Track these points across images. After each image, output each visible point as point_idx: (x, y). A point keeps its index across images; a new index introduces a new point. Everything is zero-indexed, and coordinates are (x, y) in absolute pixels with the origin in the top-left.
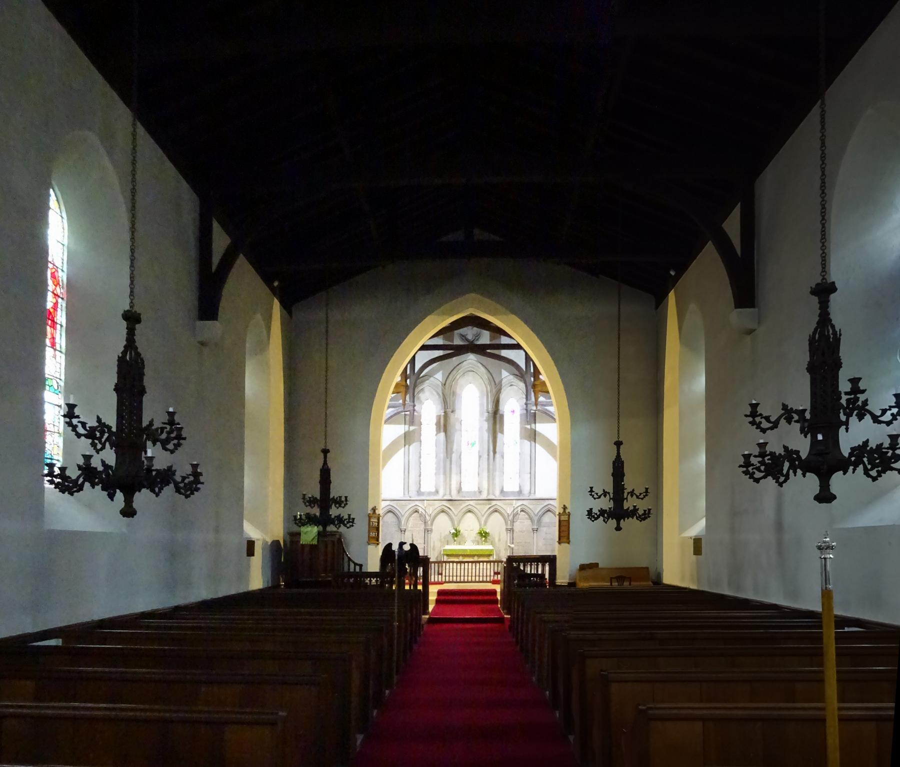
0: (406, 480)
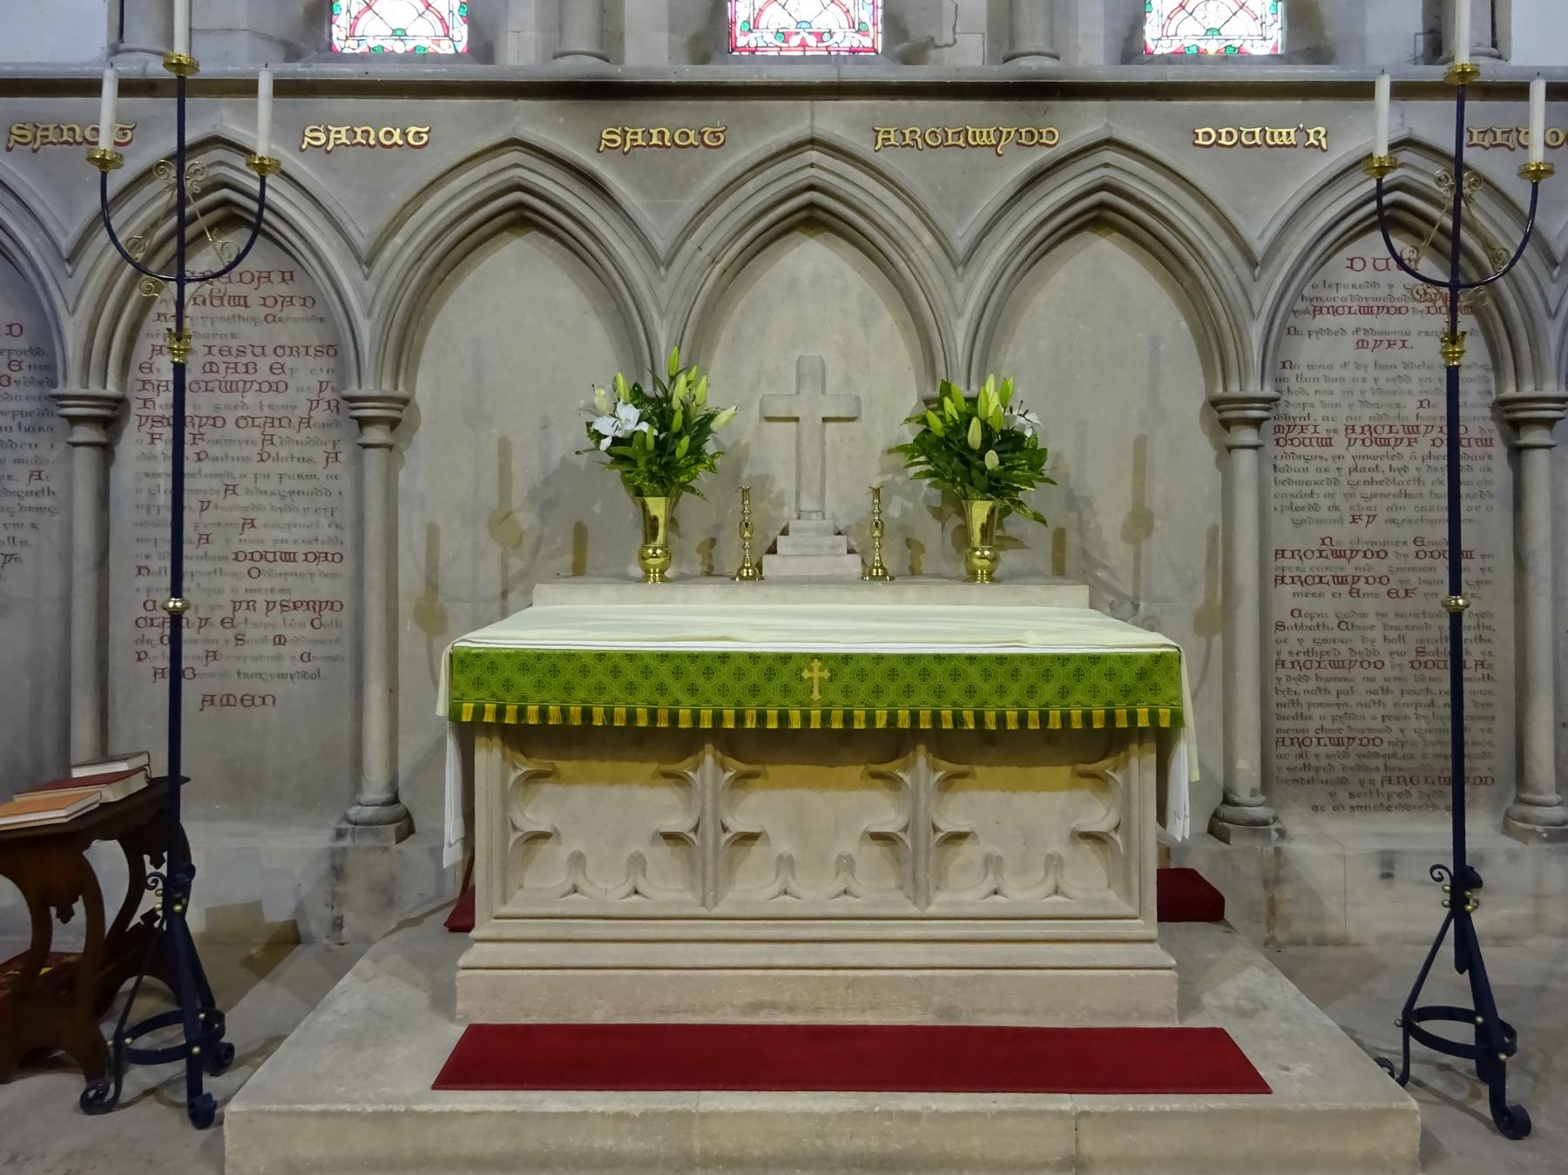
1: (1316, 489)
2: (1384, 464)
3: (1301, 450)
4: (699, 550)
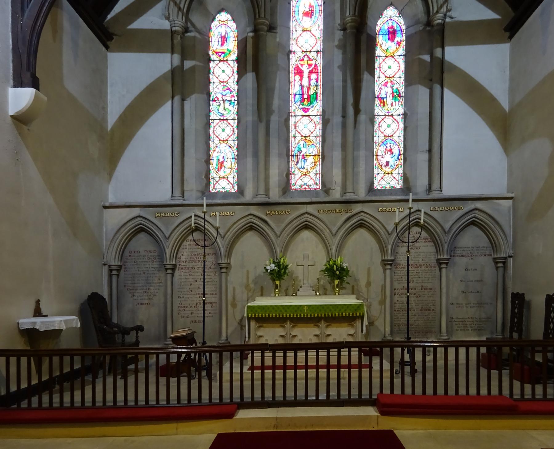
0: (177, 168)
1: (402, 277)
2: (415, 272)
3: (399, 269)
4: (284, 291)
